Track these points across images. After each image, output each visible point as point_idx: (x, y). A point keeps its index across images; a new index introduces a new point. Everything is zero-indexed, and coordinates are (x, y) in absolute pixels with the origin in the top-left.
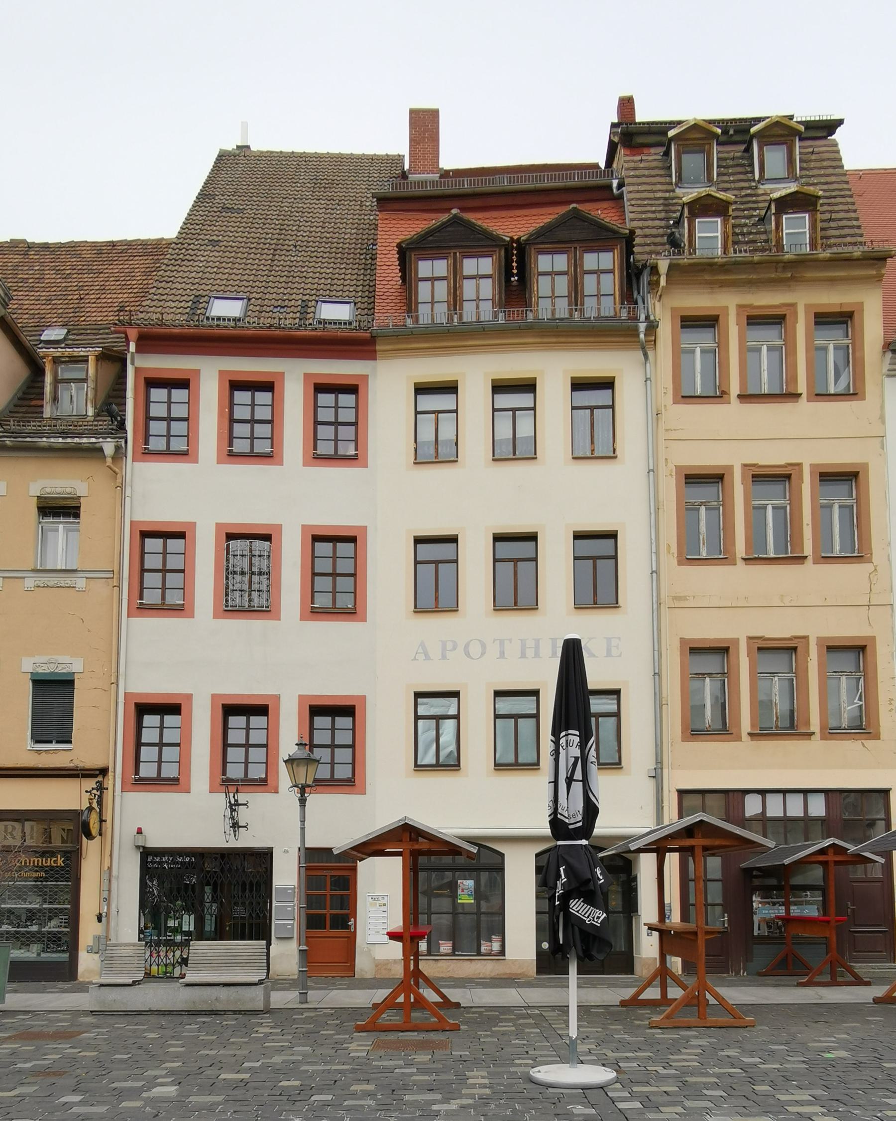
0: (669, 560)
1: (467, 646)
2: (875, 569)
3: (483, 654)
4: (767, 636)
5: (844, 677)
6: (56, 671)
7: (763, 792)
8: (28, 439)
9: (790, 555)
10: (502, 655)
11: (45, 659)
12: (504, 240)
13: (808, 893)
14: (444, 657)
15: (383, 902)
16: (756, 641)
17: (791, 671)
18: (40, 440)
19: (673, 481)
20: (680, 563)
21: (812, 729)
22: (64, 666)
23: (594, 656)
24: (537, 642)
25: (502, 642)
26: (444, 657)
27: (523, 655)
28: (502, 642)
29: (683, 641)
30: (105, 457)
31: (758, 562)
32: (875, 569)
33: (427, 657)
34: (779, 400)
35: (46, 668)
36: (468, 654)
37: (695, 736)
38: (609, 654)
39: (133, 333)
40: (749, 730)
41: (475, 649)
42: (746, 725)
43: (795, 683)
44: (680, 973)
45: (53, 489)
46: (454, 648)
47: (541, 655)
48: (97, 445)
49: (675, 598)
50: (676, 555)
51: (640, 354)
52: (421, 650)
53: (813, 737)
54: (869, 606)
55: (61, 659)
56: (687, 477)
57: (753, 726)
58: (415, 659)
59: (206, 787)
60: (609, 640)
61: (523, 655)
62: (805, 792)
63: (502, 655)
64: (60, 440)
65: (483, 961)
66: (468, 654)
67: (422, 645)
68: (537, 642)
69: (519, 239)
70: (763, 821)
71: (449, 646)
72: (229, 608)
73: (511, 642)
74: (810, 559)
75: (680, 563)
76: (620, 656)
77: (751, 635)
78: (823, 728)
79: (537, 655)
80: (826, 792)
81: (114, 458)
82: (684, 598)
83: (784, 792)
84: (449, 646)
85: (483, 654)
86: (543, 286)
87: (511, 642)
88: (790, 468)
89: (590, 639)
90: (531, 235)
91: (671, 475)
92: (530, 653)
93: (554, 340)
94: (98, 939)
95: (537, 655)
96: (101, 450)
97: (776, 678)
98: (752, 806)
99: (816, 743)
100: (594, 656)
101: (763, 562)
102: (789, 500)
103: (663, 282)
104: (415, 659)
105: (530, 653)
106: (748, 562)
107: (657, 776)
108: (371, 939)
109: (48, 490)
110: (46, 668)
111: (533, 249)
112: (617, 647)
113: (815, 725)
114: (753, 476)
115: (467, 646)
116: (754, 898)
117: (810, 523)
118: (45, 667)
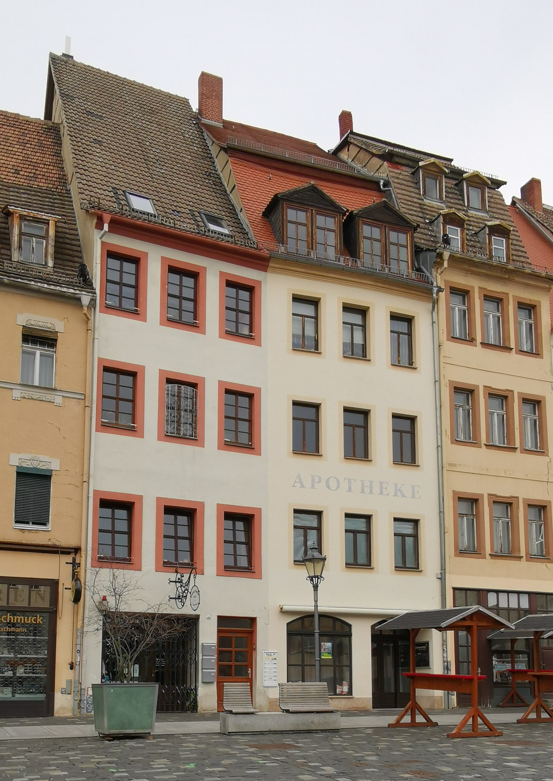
0: (447, 440)
1: (328, 481)
2: (550, 461)
3: (338, 487)
4: (498, 495)
5: (534, 524)
6: (38, 467)
7: (497, 592)
8: (19, 280)
9: (505, 446)
10: (350, 490)
11: (28, 456)
12: (343, 210)
13: (521, 656)
14: (313, 487)
15: (274, 657)
16: (492, 497)
17: (507, 518)
18: (29, 282)
19: (447, 390)
20: (452, 443)
21: (521, 555)
22: (44, 463)
23: (405, 496)
24: (371, 482)
25: (350, 481)
26: (313, 487)
27: (363, 492)
28: (350, 481)
29: (454, 492)
30: (81, 306)
31: (493, 447)
32: (550, 461)
33: (302, 486)
34: (502, 350)
35: (30, 464)
36: (328, 487)
37: (461, 554)
38: (413, 497)
39: (107, 217)
40: (490, 552)
41: (333, 484)
42: (488, 550)
43: (510, 524)
44: (456, 706)
45: (37, 322)
46: (320, 482)
47: (373, 493)
48: (77, 296)
49: (450, 465)
50: (450, 437)
51: (430, 306)
52: (298, 480)
53: (522, 559)
54: (547, 482)
55: (42, 458)
56: (455, 388)
57: (492, 549)
58: (294, 486)
59: (153, 567)
60: (413, 487)
61: (363, 492)
62: (519, 593)
63: (350, 490)
64: (46, 286)
65: (339, 699)
66: (328, 487)
67: (299, 476)
68: (371, 482)
69: (352, 212)
70: (497, 609)
71: (317, 480)
72: (169, 434)
73: (355, 481)
74: (519, 449)
75: (452, 443)
76: (420, 498)
77: (490, 493)
78: (527, 554)
79: (371, 492)
80: (529, 593)
81: (89, 307)
82: (455, 465)
83: (508, 592)
84: (317, 480)
85: (338, 487)
86: (365, 245)
87: (355, 481)
88: (507, 392)
89: (403, 485)
90: (360, 211)
91: (447, 386)
92: (367, 490)
93: (382, 285)
94: (69, 682)
95: (371, 492)
96: (79, 300)
97: (501, 521)
98: (492, 600)
99: (523, 563)
100: (405, 496)
101: (495, 448)
102: (506, 411)
103: (446, 264)
104: (294, 486)
105: (367, 490)
106: (488, 447)
107: (442, 579)
108: (266, 684)
109: (33, 322)
110: (30, 464)
111: (360, 221)
112: (418, 492)
113: (523, 553)
114: (489, 394)
115: (328, 481)
116: (493, 659)
117: (518, 428)
118: (29, 463)
